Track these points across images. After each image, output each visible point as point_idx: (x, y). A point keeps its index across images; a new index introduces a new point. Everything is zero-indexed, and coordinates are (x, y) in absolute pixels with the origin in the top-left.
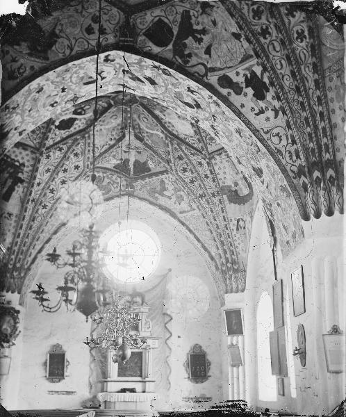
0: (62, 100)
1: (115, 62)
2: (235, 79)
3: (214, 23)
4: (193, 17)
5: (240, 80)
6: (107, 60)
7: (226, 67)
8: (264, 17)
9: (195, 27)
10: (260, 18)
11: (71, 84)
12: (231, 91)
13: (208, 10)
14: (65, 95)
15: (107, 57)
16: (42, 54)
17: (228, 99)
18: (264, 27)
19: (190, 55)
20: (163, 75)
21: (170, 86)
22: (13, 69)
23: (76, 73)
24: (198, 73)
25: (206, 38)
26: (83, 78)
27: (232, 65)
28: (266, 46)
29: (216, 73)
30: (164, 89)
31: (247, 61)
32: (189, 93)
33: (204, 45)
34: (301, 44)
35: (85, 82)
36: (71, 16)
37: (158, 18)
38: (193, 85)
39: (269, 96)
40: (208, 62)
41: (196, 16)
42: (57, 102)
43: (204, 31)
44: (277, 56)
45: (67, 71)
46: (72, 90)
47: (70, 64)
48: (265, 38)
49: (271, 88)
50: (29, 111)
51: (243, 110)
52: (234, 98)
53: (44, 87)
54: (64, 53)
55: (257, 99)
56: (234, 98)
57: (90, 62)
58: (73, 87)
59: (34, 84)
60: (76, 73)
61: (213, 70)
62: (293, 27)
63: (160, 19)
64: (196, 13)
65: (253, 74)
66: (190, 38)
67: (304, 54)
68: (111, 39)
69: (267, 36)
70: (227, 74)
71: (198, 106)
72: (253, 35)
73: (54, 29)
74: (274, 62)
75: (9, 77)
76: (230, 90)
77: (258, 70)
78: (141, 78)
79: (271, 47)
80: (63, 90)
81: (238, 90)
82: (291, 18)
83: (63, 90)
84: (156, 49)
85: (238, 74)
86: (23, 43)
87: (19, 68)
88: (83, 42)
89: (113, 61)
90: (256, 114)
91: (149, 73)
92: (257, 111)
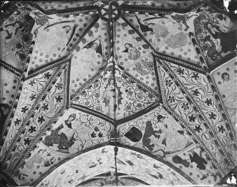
0: (76, 178)
1: (108, 152)
2: (183, 158)
3: (166, 126)
4: (153, 124)
5: (187, 158)
6: (103, 152)
7: (177, 151)
8: (196, 120)
9: (155, 129)
10: (194, 121)
11: (81, 167)
12: (182, 165)
13: (162, 120)
15: (103, 149)
16: (65, 150)
17: (181, 171)
18: (197, 126)
19: (153, 145)
20: (138, 159)
21: (142, 165)
22: (48, 161)
24: (160, 156)
25: (162, 135)
27: (180, 149)
28: (200, 137)
29: (170, 155)
30: (138, 167)
31: (190, 146)
32: (155, 169)
33: (162, 139)
34: (222, 134)
36: (82, 128)
37: (132, 126)
38: (158, 163)
39: (208, 167)
40: (165, 149)
41: (155, 123)
43: (160, 131)
44: (209, 143)
45: (80, 159)
46: (82, 171)
47: (82, 155)
48: (199, 132)
49: (208, 162)
51: (191, 177)
52: (184, 169)
53: (66, 170)
54: (78, 149)
55: (200, 169)
56: (184, 169)
58: (83, 169)
59: (60, 169)
61: (169, 153)
62: (215, 125)
63: (134, 127)
64: (154, 122)
65: (195, 154)
66: (152, 135)
67: (226, 140)
68: (106, 139)
69: (200, 131)
70: (178, 155)
71: (161, 176)
72: (191, 130)
73: (74, 135)
74: (207, 145)
75: (45, 165)
76: (181, 165)
77: (198, 151)
78: (124, 161)
79: (204, 137)
80: (77, 172)
81: (187, 164)
82: (213, 120)
83: (77, 172)
84: (132, 144)
85: (185, 154)
86: (55, 145)
87: (52, 159)
88: (89, 142)
89: (107, 152)
90: (201, 179)
91: (129, 158)
92: (201, 177)
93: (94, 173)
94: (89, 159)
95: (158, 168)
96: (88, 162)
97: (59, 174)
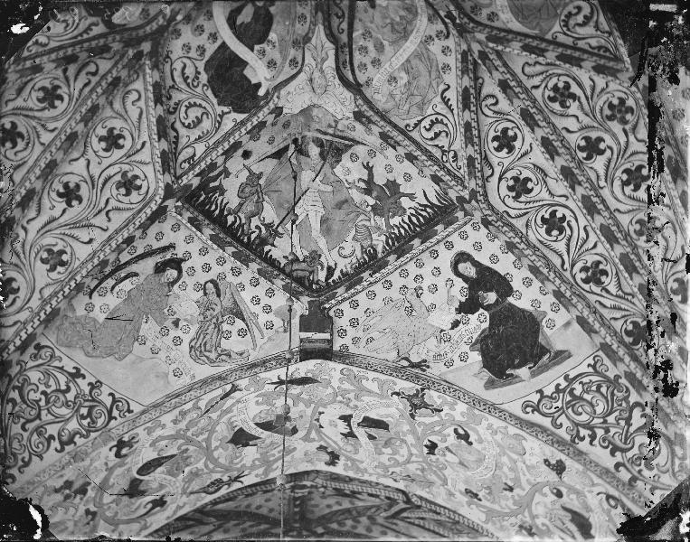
11: (414, 451)
14: (434, 433)
23: (397, 464)
26: (387, 444)
35: (382, 432)
42: (456, 431)
50: (511, 489)
57: (366, 470)
58: (410, 439)
60: (397, 464)
78: (264, 434)
91: (250, 453)
93: (374, 387)
94: (384, 459)
95: (150, 506)
96: (388, 451)
97: (484, 502)
